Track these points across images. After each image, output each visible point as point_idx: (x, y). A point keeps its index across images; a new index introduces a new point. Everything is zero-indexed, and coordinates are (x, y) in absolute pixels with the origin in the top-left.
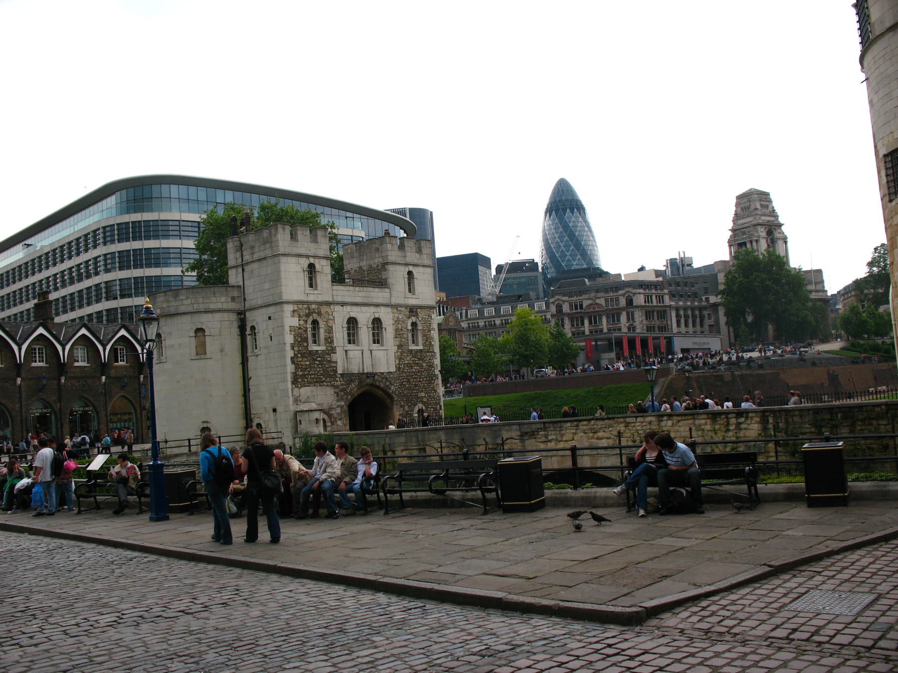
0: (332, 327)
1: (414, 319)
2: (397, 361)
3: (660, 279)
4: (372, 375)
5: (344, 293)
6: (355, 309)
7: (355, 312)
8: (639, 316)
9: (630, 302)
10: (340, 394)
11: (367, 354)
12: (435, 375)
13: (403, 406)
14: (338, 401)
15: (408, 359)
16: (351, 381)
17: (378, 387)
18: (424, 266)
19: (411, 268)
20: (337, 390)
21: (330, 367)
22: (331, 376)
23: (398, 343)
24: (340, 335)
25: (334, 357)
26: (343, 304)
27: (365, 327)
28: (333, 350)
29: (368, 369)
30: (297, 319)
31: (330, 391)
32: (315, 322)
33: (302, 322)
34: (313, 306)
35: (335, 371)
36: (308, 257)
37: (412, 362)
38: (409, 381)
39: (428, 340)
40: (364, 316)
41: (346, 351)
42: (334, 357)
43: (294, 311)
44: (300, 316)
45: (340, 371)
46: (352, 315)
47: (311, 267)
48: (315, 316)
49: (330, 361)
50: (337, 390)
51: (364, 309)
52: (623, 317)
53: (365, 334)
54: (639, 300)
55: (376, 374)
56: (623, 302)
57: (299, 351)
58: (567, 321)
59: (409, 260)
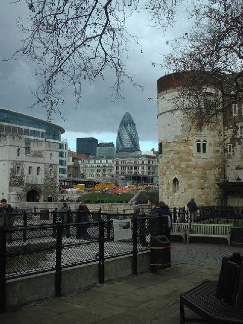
3: (155, 155)
4: (35, 185)
5: (28, 158)
7: (32, 165)
8: (146, 168)
9: (143, 163)
15: (48, 181)
19: (52, 152)
24: (26, 172)
28: (23, 176)
31: (21, 189)
32: (18, 167)
37: (50, 181)
40: (35, 166)
47: (19, 149)
48: (19, 165)
52: (140, 168)
54: (146, 162)
56: (140, 162)
58: (120, 168)
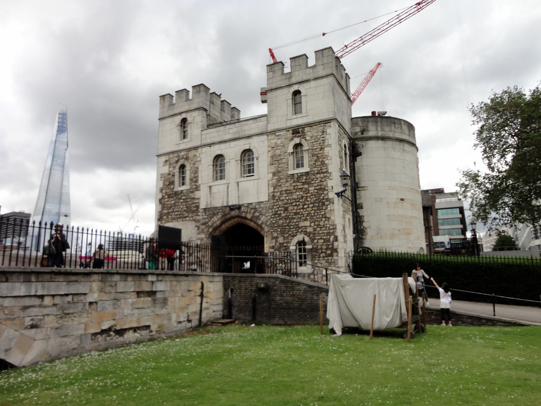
0: (197, 168)
1: (297, 140)
2: (272, 189)
4: (239, 207)
6: (223, 146)
11: (233, 186)
12: (328, 200)
13: (276, 238)
14: (199, 234)
16: (214, 214)
17: (246, 218)
18: (316, 79)
20: (198, 224)
21: (194, 203)
22: (193, 212)
23: (273, 169)
25: (197, 194)
26: (210, 145)
27: (233, 163)
28: (197, 188)
29: (233, 201)
30: (167, 167)
32: (183, 167)
33: (171, 169)
34: (183, 153)
35: (198, 207)
36: (181, 113)
38: (286, 209)
40: (232, 152)
41: (210, 187)
43: (166, 161)
44: (170, 164)
45: (202, 206)
46: (219, 152)
49: (193, 198)
50: (198, 224)
51: (233, 144)
53: (233, 168)
55: (243, 205)
57: (166, 193)
59: (294, 80)
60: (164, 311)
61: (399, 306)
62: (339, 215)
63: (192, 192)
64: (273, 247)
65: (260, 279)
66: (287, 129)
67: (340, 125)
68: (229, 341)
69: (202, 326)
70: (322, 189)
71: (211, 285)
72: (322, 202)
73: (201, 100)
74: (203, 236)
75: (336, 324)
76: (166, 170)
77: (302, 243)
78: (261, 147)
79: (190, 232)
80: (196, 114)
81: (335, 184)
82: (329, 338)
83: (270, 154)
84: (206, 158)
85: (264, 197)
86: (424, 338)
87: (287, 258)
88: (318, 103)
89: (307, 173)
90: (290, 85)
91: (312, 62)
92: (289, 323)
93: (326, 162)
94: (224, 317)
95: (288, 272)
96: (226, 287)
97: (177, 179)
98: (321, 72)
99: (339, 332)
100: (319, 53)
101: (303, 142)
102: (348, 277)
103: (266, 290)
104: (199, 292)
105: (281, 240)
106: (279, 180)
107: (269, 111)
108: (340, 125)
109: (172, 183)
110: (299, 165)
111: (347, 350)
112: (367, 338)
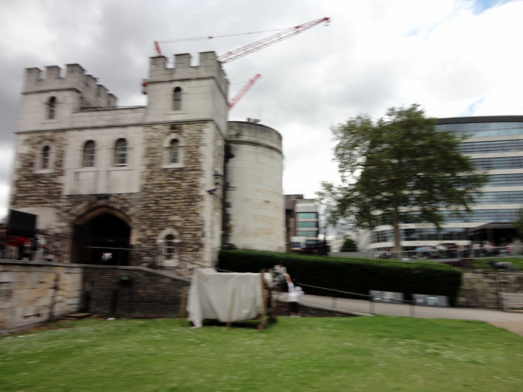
1: (174, 136)
4: (106, 197)
10: (62, 213)
11: (103, 175)
12: (200, 197)
14: (59, 221)
15: (160, 179)
17: (113, 208)
18: (198, 79)
25: (61, 179)
28: (61, 173)
29: (102, 190)
38: (157, 203)
39: (194, 157)
40: (105, 140)
42: (61, 179)
46: (90, 138)
50: (58, 211)
53: (104, 156)
59: (176, 76)
60: (6, 305)
61: (255, 300)
62: (208, 213)
63: (55, 177)
64: (139, 240)
65: (123, 271)
66: (164, 124)
67: (217, 128)
68: (82, 336)
69: (53, 321)
70: (194, 186)
71: (67, 277)
72: (192, 198)
73: (74, 81)
74: (63, 224)
75: (196, 315)
76: (26, 149)
77: (170, 237)
78: (136, 138)
79: (47, 219)
80: (67, 94)
81: (207, 182)
82: (188, 330)
83: (146, 146)
84: (74, 143)
85: (135, 189)
86: (275, 328)
87: (154, 251)
88: (197, 102)
89: (181, 169)
90: (171, 81)
91: (195, 62)
92: (151, 316)
93: (201, 160)
94: (80, 311)
95: (153, 265)
96: (85, 279)
97: (38, 161)
98: (203, 73)
99: (198, 324)
100: (204, 55)
101: (181, 139)
102: (211, 272)
103: (128, 283)
104: (52, 284)
105: (149, 233)
106: (152, 173)
107: (150, 103)
108: (217, 128)
109: (31, 165)
110: (174, 160)
111: (204, 341)
112: (224, 329)
